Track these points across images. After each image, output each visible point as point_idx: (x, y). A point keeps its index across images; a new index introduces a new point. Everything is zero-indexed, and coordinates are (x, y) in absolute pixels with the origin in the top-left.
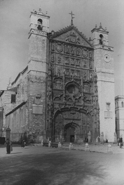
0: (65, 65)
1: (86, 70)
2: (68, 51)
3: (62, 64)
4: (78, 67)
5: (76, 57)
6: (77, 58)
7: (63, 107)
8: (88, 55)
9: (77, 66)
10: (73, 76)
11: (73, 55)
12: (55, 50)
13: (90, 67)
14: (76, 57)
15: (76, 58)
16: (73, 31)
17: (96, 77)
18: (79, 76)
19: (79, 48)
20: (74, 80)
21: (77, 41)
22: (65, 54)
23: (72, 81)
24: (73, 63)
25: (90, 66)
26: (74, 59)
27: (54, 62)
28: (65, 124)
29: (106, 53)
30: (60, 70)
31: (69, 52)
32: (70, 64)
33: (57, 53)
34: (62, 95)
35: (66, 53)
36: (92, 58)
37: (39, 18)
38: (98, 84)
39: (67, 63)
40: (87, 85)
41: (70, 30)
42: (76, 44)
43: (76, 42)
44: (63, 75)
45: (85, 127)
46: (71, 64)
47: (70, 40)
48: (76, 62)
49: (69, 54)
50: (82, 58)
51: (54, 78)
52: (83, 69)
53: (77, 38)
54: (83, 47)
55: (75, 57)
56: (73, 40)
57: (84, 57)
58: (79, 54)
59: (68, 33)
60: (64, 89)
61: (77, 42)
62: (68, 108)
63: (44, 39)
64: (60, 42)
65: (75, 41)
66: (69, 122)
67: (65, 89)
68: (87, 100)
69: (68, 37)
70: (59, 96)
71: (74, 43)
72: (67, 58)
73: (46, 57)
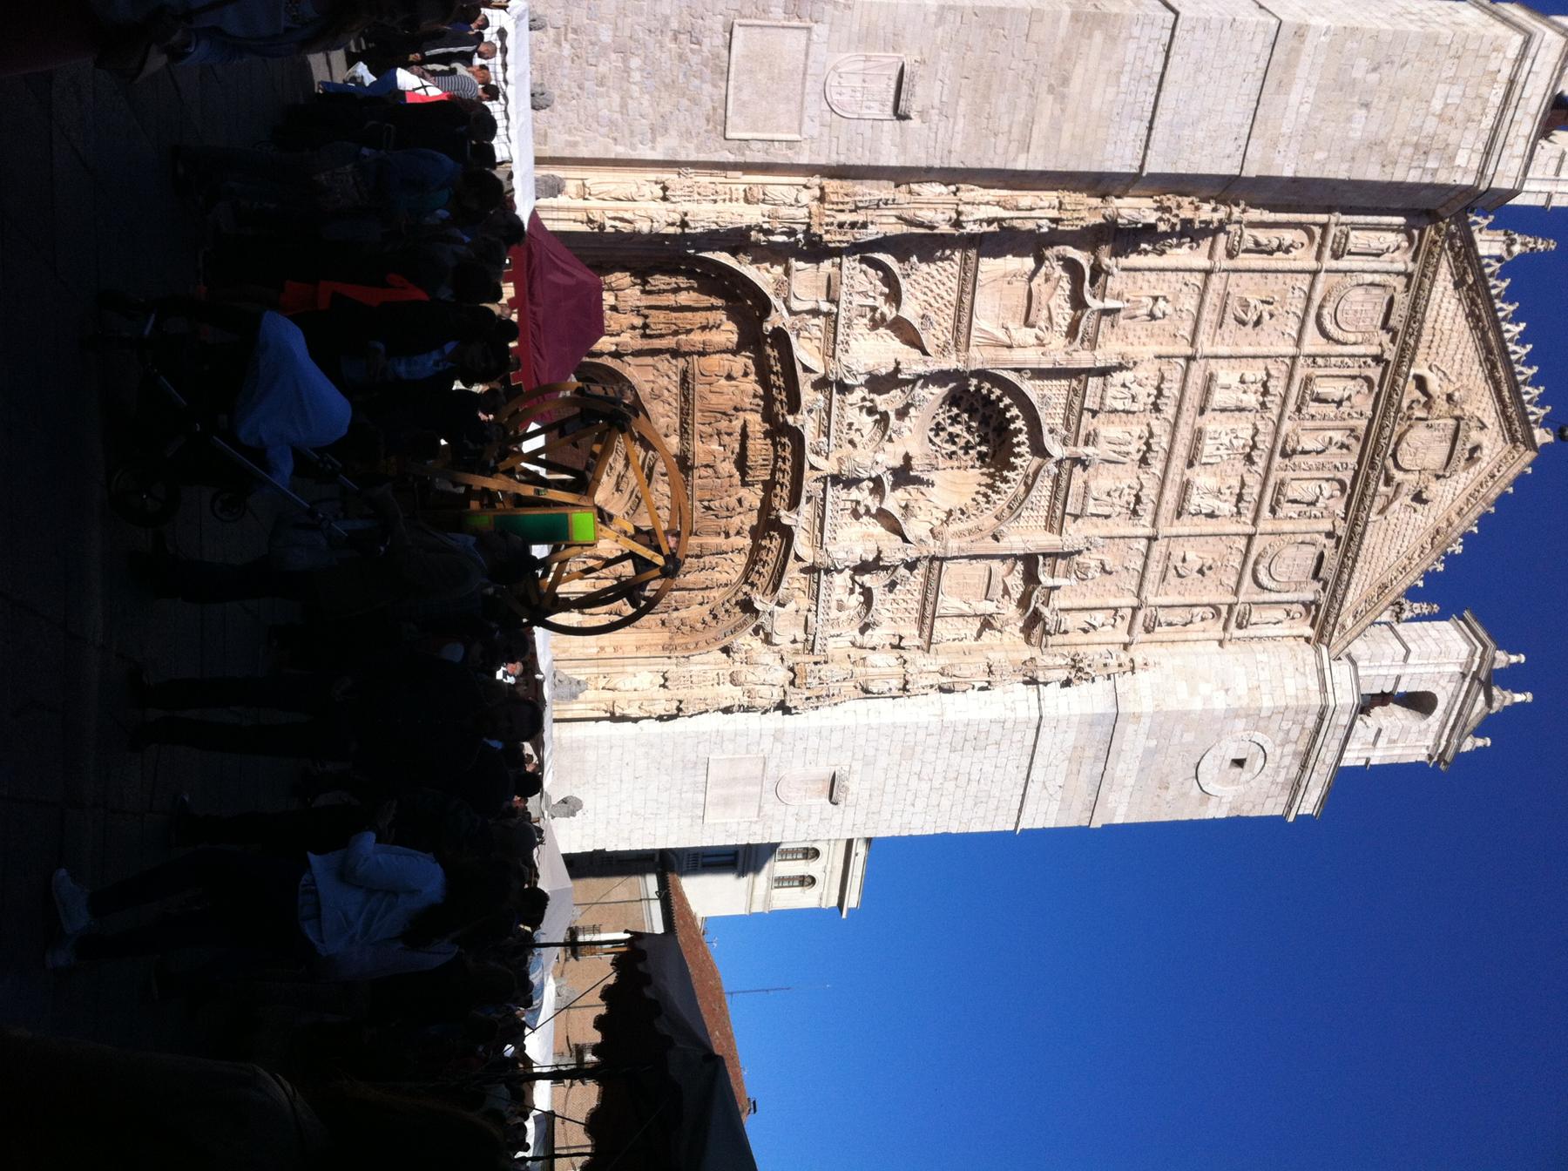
0: (1197, 372)
1: (1142, 576)
2: (1319, 399)
3: (1205, 346)
4: (1171, 495)
6: (1257, 490)
9: (1186, 487)
10: (1090, 450)
11: (1284, 454)
13: (1163, 615)
15: (1254, 483)
16: (1492, 443)
17: (1077, 672)
18: (1091, 509)
19: (1339, 509)
20: (1059, 463)
21: (1405, 489)
24: (1208, 447)
25: (1178, 616)
26: (1249, 459)
30: (1152, 316)
32: (1200, 422)
34: (906, 333)
35: (1308, 380)
36: (1240, 626)
38: (1014, 700)
39: (1219, 398)
40: (1006, 592)
43: (1398, 476)
46: (1198, 435)
47: (1423, 414)
50: (1250, 537)
51: (1084, 262)
52: (1149, 548)
53: (1435, 489)
54: (1349, 542)
55: (1268, 469)
56: (1423, 447)
57: (1256, 563)
58: (1287, 509)
59: (1482, 405)
61: (1390, 491)
63: (1461, 160)
67: (982, 375)
69: (1450, 397)
70: (910, 310)
73: (1288, 173)
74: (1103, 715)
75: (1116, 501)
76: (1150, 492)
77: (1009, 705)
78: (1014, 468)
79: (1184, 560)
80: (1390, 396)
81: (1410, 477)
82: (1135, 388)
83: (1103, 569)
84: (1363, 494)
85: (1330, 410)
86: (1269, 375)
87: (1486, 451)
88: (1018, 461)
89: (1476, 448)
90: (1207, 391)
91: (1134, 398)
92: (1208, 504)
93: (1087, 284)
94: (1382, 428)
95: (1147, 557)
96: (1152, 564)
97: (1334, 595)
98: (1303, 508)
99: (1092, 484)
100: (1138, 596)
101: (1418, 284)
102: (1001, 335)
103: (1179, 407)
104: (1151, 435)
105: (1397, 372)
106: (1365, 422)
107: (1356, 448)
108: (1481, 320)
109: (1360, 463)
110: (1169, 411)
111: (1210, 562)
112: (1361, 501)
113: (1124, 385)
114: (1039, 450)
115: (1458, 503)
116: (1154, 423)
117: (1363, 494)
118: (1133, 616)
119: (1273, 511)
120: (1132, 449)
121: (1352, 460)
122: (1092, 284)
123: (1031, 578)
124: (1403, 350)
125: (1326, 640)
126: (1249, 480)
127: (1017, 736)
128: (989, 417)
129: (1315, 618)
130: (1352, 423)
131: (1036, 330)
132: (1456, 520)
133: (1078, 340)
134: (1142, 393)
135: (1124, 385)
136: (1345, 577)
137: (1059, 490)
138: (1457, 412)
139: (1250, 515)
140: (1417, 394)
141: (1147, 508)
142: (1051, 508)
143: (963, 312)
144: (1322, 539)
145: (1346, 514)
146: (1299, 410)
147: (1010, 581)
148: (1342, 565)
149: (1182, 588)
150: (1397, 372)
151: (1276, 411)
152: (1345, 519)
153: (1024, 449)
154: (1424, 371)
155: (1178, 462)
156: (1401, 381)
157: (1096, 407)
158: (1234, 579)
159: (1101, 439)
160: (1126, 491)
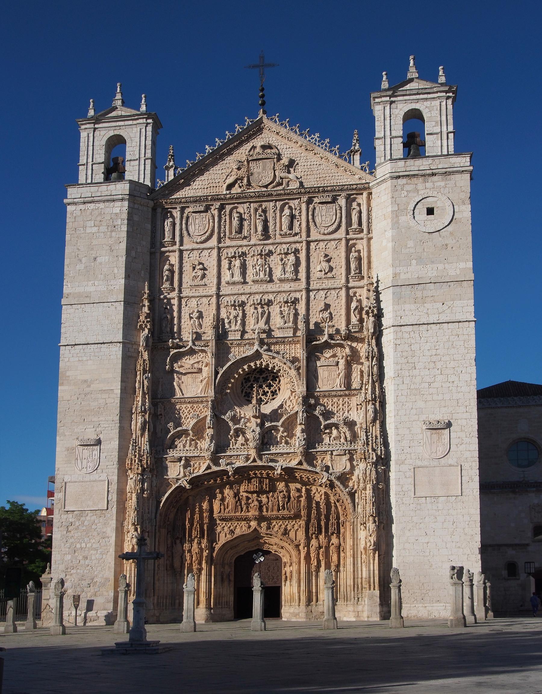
4: (286, 287)
5: (281, 243)
6: (284, 246)
7: (201, 468)
8: (341, 222)
9: (281, 280)
12: (177, 239)
14: (281, 243)
22: (228, 243)
23: (250, 352)
27: (173, 290)
28: (223, 539)
29: (423, 193)
31: (245, 232)
33: (186, 250)
36: (362, 231)
37: (111, 133)
40: (334, 356)
41: (247, 140)
42: (278, 188)
44: (209, 334)
45: (320, 547)
48: (280, 268)
49: (245, 242)
55: (273, 244)
59: (242, 153)
60: (211, 393)
62: (225, 472)
64: (197, 200)
65: (270, 180)
66: (241, 529)
68: (328, 427)
69: (239, 169)
71: (266, 186)
72: (232, 257)
74: (394, 293)
75: (286, 312)
76: (282, 298)
77: (388, 344)
78: (268, 365)
79: (321, 271)
80: (236, 198)
81: (277, 174)
82: (231, 317)
83: (324, 310)
84: (285, 194)
85: (246, 223)
86: (227, 257)
87: (263, 143)
88: (264, 364)
89: (264, 147)
90: (234, 283)
91: (236, 317)
92: (290, 268)
93: (181, 350)
94: (251, 197)
95: (319, 290)
96: (324, 286)
97: (341, 190)
98: (295, 221)
99: (278, 326)
100: (341, 288)
101: (184, 204)
102: (204, 382)
103: (241, 294)
104: (254, 304)
105: (225, 199)
106: (252, 205)
107: (264, 205)
108: (201, 168)
109: (272, 201)
110: (244, 298)
111: (322, 259)
112: (288, 194)
113: (230, 322)
114: (257, 355)
115: (293, 145)
116: (249, 304)
117: (285, 194)
118: (353, 288)
119: (296, 234)
120: (260, 310)
121: (272, 204)
122: (181, 347)
123: (327, 345)
124: (215, 200)
125: (366, 186)
126: (278, 252)
127: (406, 336)
128: (245, 382)
129: (357, 194)
130: (252, 210)
131: (203, 367)
132: (299, 143)
133: (206, 349)
134: (234, 313)
135: (230, 322)
136: (329, 188)
137: (283, 341)
138: (246, 163)
139: (298, 245)
140: (237, 186)
141: (294, 295)
142: (290, 343)
143: (194, 401)
144: (311, 206)
145: (298, 198)
146: (245, 238)
147: (328, 355)
148: (324, 191)
149: (338, 267)
150: (225, 199)
151: (245, 249)
152: (300, 198)
153: (258, 362)
154: (225, 186)
155: (270, 287)
156: (228, 196)
157: (240, 333)
158: (333, 242)
159: (254, 328)
160: (283, 308)
